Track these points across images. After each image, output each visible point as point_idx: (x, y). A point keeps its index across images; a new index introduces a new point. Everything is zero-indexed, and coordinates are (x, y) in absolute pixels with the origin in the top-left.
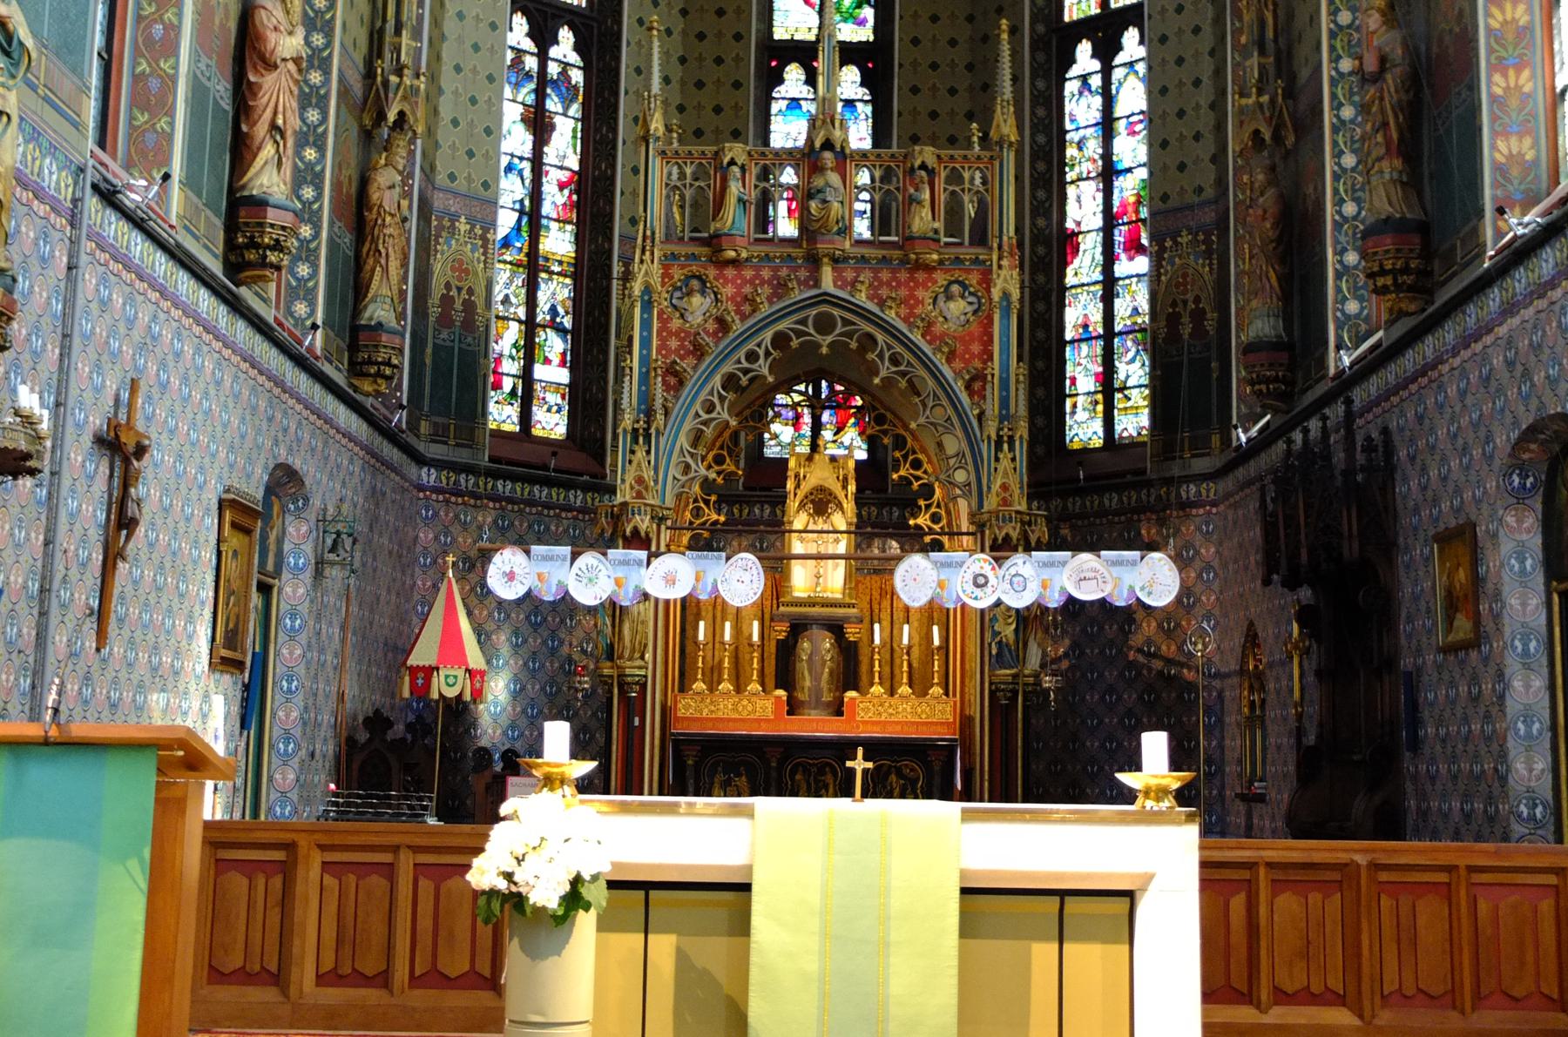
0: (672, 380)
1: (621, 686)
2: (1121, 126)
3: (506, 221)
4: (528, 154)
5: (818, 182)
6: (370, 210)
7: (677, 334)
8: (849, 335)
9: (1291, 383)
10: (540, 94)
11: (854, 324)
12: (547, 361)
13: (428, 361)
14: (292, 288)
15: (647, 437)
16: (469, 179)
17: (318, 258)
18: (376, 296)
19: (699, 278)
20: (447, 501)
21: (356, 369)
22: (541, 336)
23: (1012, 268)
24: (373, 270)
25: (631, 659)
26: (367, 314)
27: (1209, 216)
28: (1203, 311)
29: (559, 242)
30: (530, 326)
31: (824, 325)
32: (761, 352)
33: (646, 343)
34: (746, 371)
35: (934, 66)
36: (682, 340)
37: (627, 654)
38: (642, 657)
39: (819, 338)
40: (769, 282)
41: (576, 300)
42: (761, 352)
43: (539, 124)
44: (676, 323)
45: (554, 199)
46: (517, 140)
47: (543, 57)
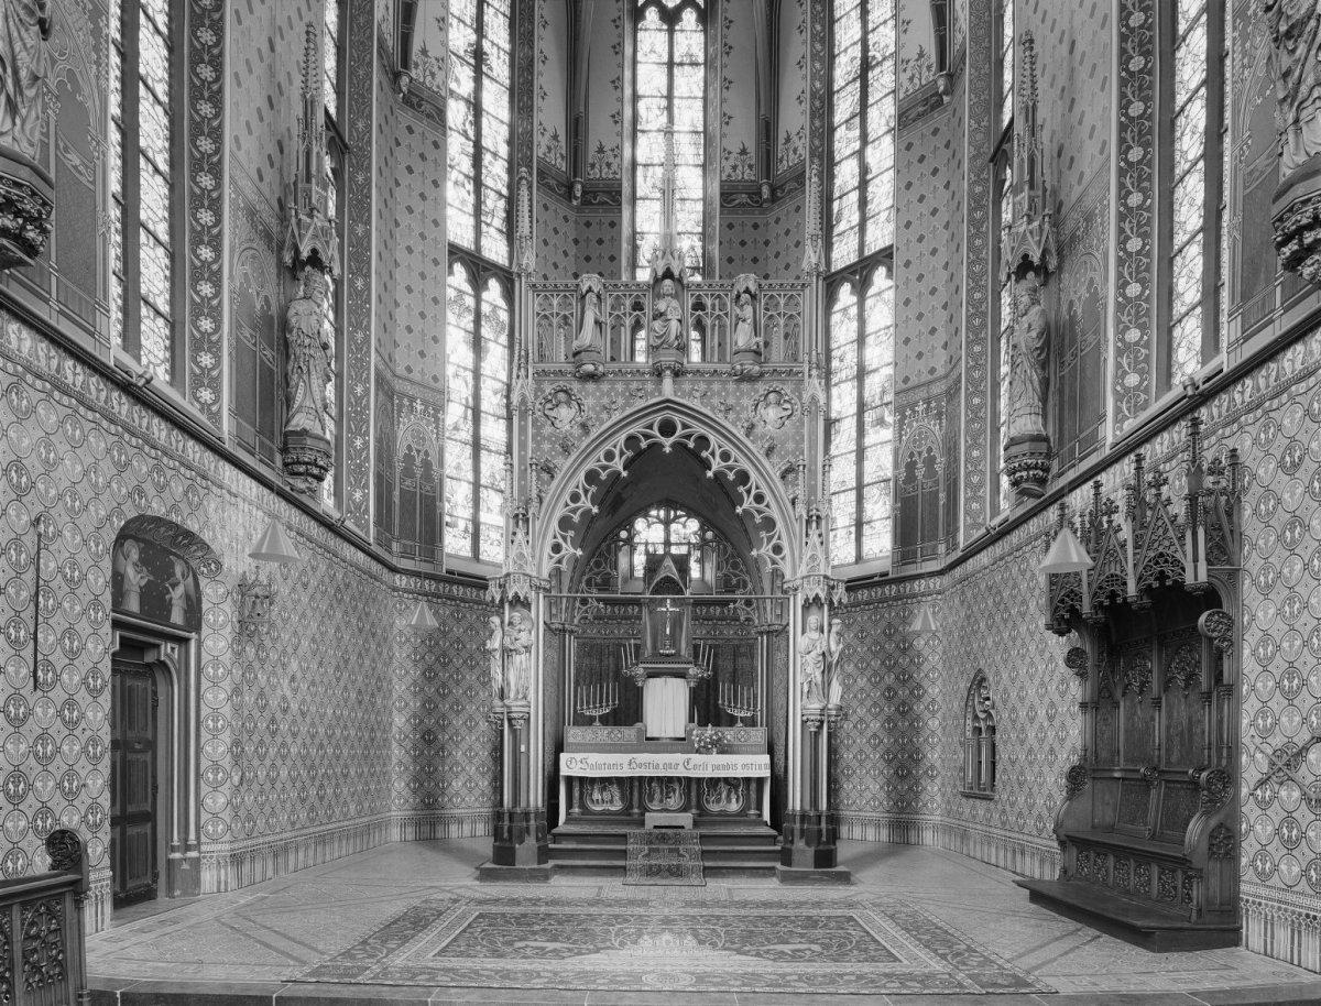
0: (545, 476)
1: (510, 720)
2: (870, 340)
4: (471, 366)
6: (291, 332)
7: (549, 439)
8: (688, 437)
9: (1046, 470)
11: (689, 427)
13: (397, 500)
14: (195, 375)
15: (527, 521)
16: (422, 372)
17: (220, 349)
18: (301, 406)
19: (566, 392)
20: (416, 599)
21: (289, 468)
22: (484, 493)
23: (819, 377)
24: (297, 385)
25: (516, 699)
26: (294, 422)
27: (938, 389)
28: (934, 458)
31: (667, 428)
32: (617, 452)
34: (604, 468)
36: (553, 443)
37: (512, 695)
38: (525, 697)
39: (663, 439)
40: (623, 394)
42: (617, 452)
44: (548, 430)
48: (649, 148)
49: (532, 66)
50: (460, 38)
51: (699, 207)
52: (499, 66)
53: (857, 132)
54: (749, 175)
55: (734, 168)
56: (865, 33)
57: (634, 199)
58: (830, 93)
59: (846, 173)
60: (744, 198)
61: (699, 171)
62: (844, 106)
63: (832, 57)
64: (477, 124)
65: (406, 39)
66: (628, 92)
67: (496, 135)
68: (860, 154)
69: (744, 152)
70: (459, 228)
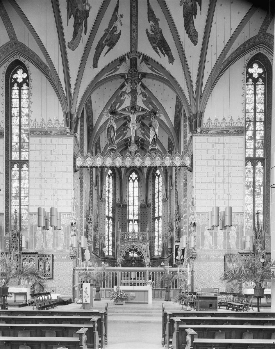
3: (106, 237)
5: (133, 235)
10: (109, 225)
12: (110, 249)
29: (111, 238)
30: (109, 246)
33: (119, 249)
35: (143, 221)
41: (112, 243)
43: (109, 228)
45: (110, 234)
46: (107, 229)
47: (109, 222)
48: (131, 199)
49: (115, 191)
50: (107, 189)
51: (138, 206)
52: (111, 191)
53: (158, 200)
54: (144, 203)
55: (142, 202)
56: (159, 187)
57: (129, 206)
58: (155, 194)
59: (156, 205)
60: (143, 206)
61: (137, 202)
62: (156, 196)
63: (155, 189)
64: (109, 199)
65: (102, 194)
66: (128, 191)
67: (111, 200)
68: (158, 202)
69: (143, 200)
70: (107, 214)
